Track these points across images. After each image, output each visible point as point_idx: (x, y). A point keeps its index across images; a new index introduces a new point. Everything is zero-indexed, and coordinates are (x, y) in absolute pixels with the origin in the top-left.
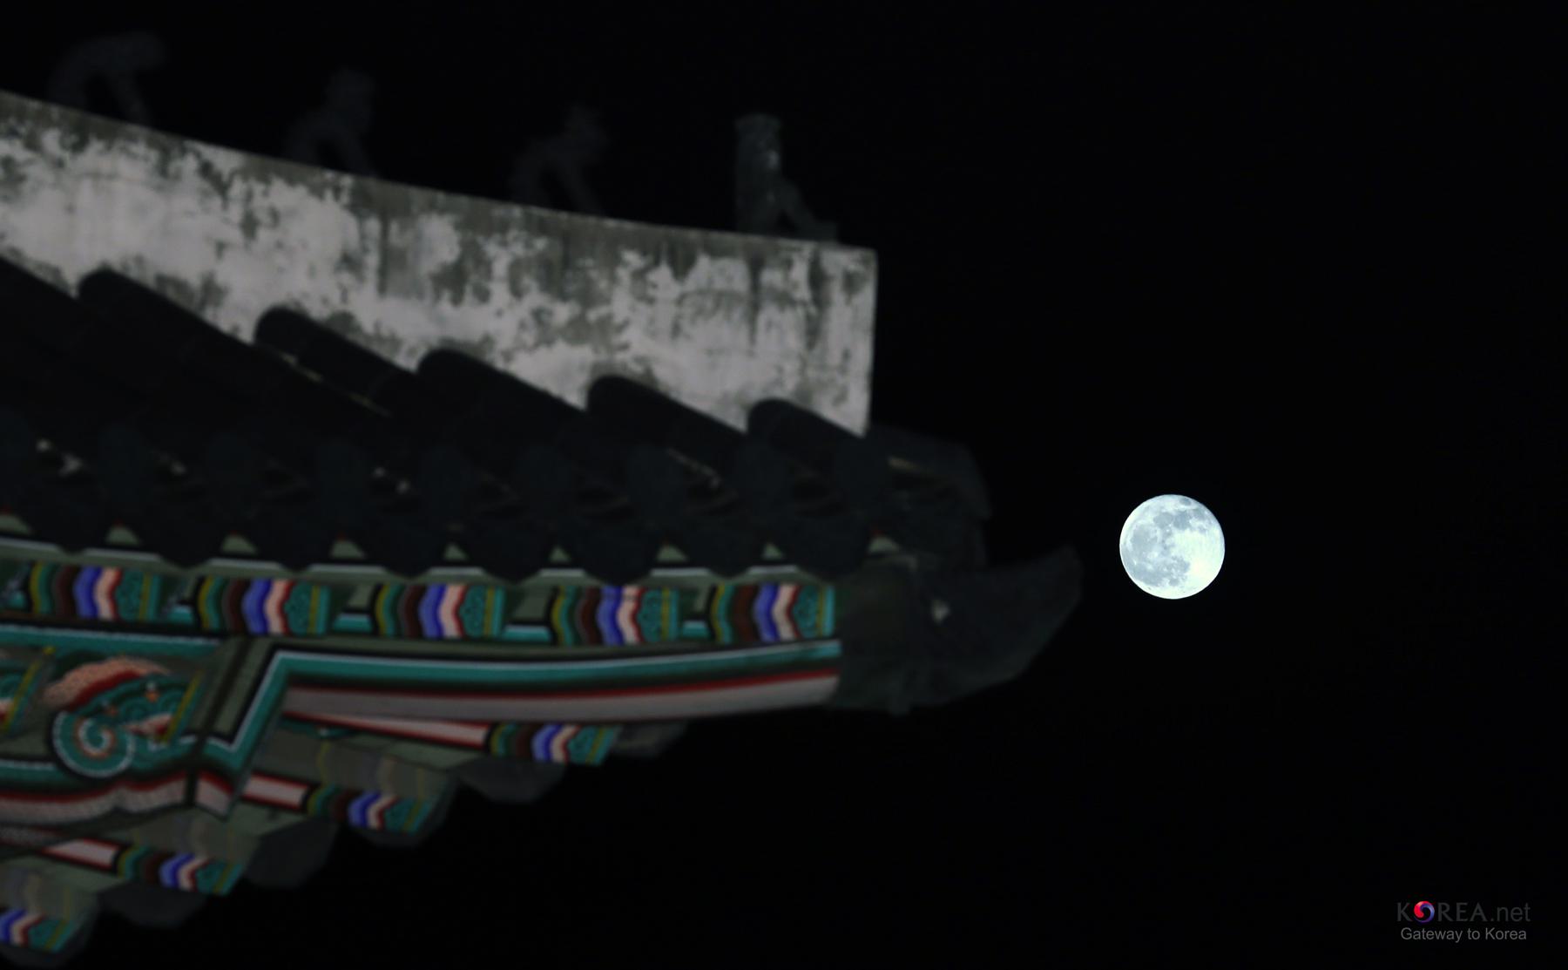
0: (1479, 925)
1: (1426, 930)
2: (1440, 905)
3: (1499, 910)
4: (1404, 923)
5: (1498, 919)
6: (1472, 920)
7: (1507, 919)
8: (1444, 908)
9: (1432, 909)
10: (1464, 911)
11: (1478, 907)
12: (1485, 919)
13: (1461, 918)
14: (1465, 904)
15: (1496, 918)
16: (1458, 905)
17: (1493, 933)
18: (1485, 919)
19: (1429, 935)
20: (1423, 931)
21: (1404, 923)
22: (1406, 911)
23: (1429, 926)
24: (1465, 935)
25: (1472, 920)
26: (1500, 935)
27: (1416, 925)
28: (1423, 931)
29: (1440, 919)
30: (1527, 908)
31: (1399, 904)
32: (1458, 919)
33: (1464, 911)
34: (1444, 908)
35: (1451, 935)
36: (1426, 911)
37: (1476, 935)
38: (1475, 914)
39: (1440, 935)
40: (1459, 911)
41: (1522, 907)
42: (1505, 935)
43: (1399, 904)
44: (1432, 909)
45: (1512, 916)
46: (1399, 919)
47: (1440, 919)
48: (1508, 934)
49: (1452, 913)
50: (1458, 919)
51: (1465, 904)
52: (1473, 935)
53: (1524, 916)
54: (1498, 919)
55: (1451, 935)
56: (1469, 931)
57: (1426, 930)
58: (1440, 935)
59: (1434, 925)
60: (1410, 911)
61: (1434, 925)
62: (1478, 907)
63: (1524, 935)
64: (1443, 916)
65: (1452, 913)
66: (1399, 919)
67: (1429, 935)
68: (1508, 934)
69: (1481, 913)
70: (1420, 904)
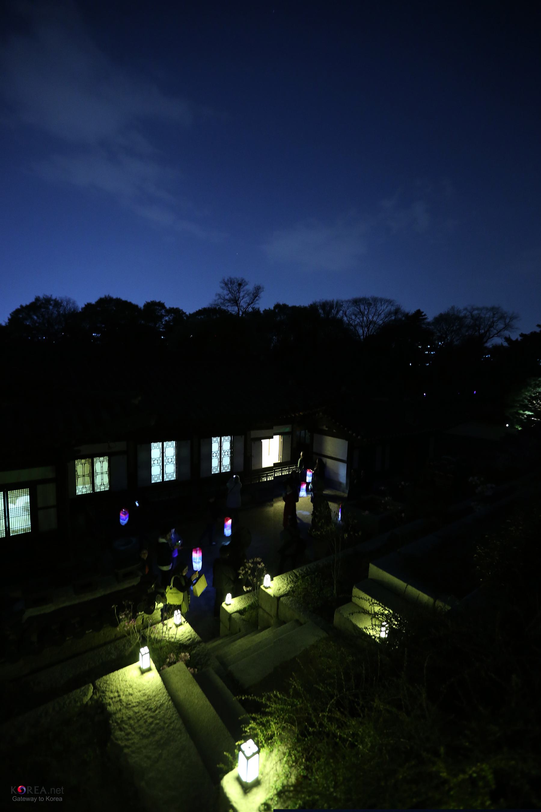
0: (43, 795)
1: (23, 797)
2: (28, 787)
3: (51, 789)
4: (14, 794)
5: (51, 793)
6: (41, 793)
7: (54, 793)
8: (29, 788)
9: (25, 789)
10: (38, 790)
11: (43, 788)
12: (46, 793)
13: (36, 792)
14: (38, 787)
15: (50, 793)
16: (35, 787)
17: (49, 798)
18: (46, 793)
19: (24, 799)
20: (21, 798)
21: (14, 794)
22: (14, 790)
24: (38, 799)
25: (41, 793)
27: (18, 795)
28: (21, 798)
29: (28, 793)
30: (62, 789)
31: (12, 787)
32: (35, 793)
33: (38, 790)
34: (29, 788)
35: (32, 799)
36: (22, 790)
37: (42, 799)
38: (42, 791)
39: (28, 799)
40: (35, 790)
41: (60, 788)
42: (53, 799)
43: (12, 787)
44: (25, 789)
45: (57, 792)
46: (12, 793)
47: (28, 793)
48: (55, 799)
49: (33, 791)
50: (35, 793)
51: (38, 787)
52: (41, 799)
53: (61, 792)
54: (51, 793)
55: (32, 799)
56: (40, 798)
57: (23, 797)
58: (28, 799)
59: (26, 795)
60: (16, 790)
61: (26, 795)
62: (43, 788)
63: (61, 799)
64: (29, 791)
65: (33, 791)
66: (12, 793)
67: (24, 799)
68: (55, 799)
69: (44, 791)
70: (20, 787)
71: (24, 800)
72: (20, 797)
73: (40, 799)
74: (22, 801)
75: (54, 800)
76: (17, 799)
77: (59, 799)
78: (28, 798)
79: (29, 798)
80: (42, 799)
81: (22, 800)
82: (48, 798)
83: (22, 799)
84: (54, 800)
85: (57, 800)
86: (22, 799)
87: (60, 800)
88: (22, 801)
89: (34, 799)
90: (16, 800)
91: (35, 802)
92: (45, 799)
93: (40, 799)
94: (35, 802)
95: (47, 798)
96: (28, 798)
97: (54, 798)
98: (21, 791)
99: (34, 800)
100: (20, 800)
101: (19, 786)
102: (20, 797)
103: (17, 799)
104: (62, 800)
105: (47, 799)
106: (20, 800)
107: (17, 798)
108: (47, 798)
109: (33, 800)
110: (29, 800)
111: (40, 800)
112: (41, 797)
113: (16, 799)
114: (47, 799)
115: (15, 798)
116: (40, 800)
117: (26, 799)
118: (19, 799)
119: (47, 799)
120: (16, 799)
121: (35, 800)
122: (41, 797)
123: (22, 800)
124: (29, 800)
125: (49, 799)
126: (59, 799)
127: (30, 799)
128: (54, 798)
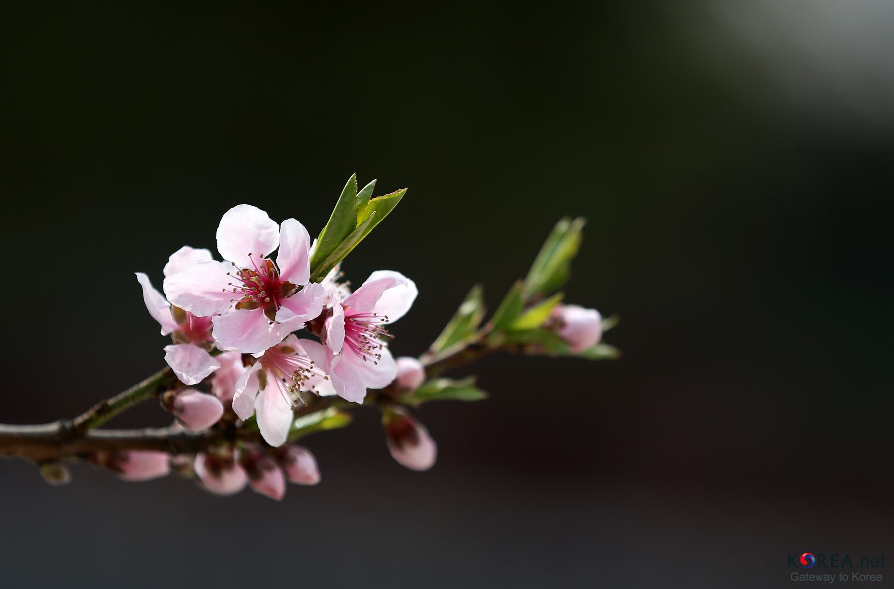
1: (809, 574)
9: (813, 559)
17: (858, 576)
19: (811, 577)
20: (807, 575)
24: (837, 577)
26: (862, 578)
28: (807, 575)
36: (808, 559)
37: (845, 578)
44: (813, 559)
48: (869, 577)
56: (840, 575)
57: (809, 574)
67: (811, 577)
68: (869, 577)
70: (804, 555)
71: (812, 579)
72: (805, 574)
73: (842, 576)
74: (807, 580)
75: (867, 580)
76: (799, 577)
77: (876, 577)
78: (819, 575)
79: (821, 577)
81: (808, 578)
82: (855, 576)
83: (808, 576)
84: (867, 580)
85: (872, 579)
86: (808, 576)
87: (879, 579)
88: (807, 580)
89: (830, 576)
90: (796, 578)
91: (831, 582)
92: (850, 576)
94: (831, 582)
95: (854, 574)
96: (819, 575)
97: (867, 576)
98: (805, 563)
100: (804, 579)
101: (815, 556)
102: (805, 574)
103: (799, 577)
104: (881, 579)
105: (855, 578)
108: (854, 574)
110: (821, 580)
111: (842, 579)
112: (842, 574)
113: (798, 577)
114: (855, 578)
115: (796, 575)
116: (842, 579)
117: (815, 578)
118: (804, 577)
119: (853, 577)
120: (798, 577)
121: (833, 580)
122: (842, 574)
123: (808, 578)
124: (821, 580)
125: (859, 579)
126: (876, 577)
127: (823, 578)
128: (867, 576)
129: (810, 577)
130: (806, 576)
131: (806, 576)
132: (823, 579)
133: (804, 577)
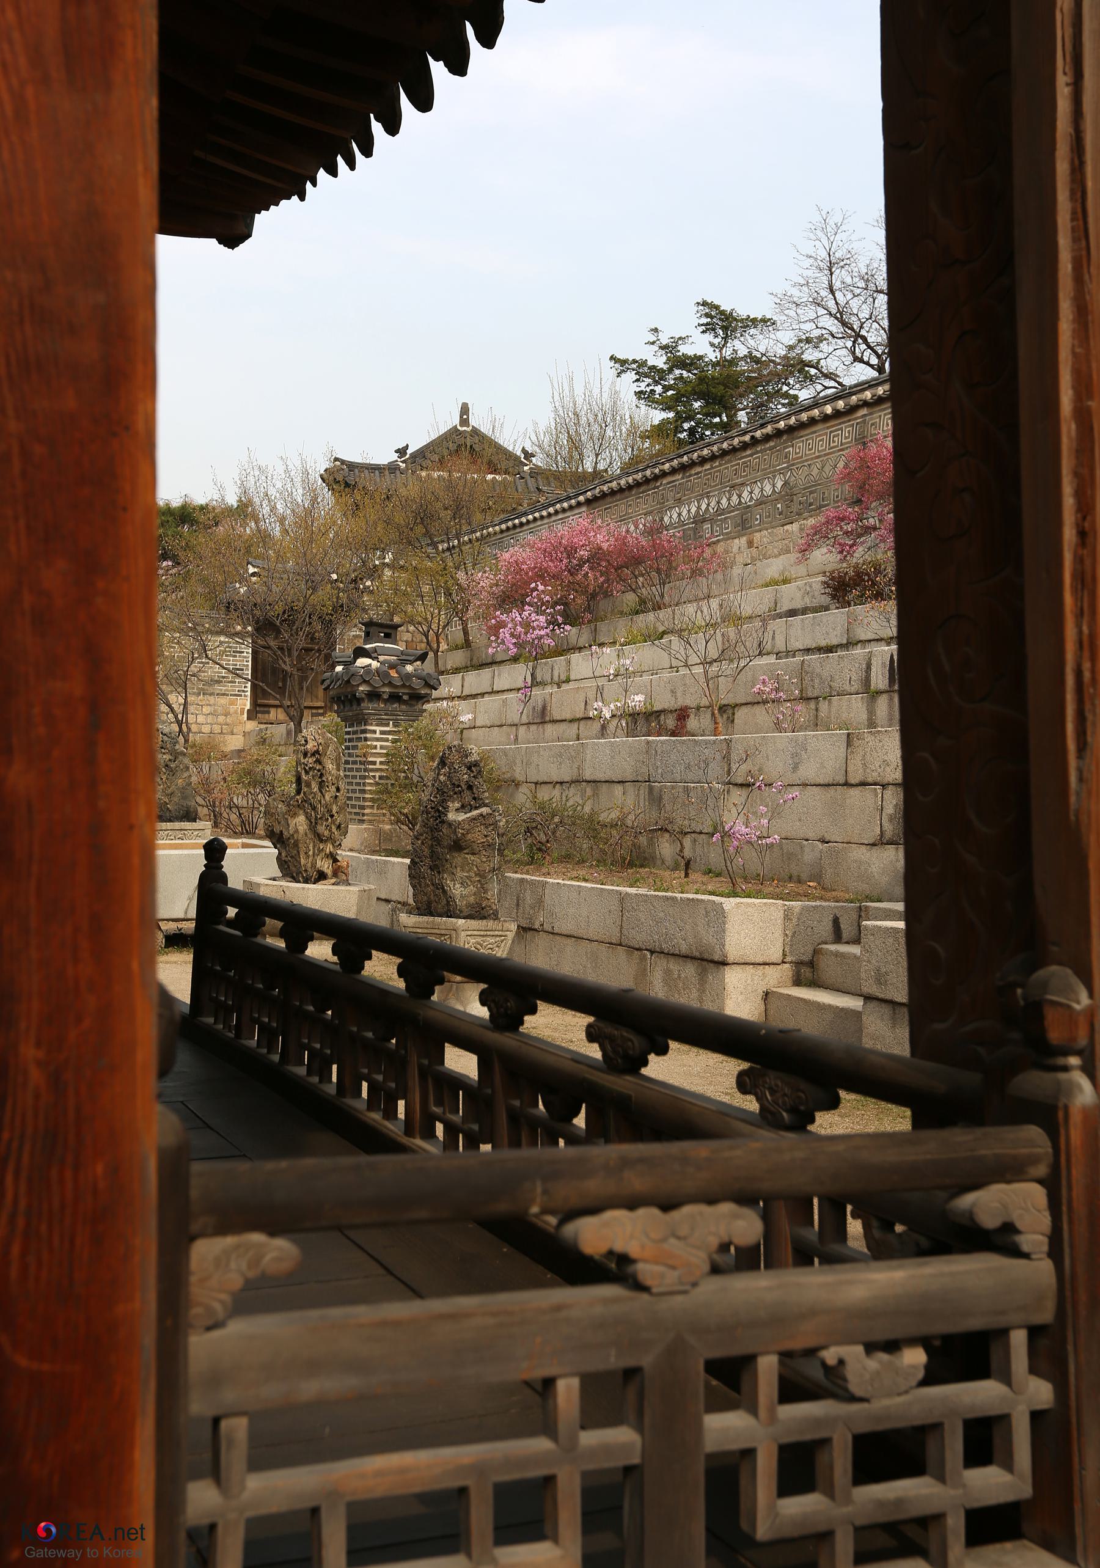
1: (49, 1549)
9: (53, 1529)
17: (111, 1551)
19: (51, 1553)
20: (46, 1550)
23: (50, 1546)
24: (84, 1555)
26: (117, 1553)
27: (39, 1544)
28: (46, 1550)
36: (48, 1531)
37: (95, 1553)
44: (53, 1529)
48: (125, 1552)
56: (88, 1550)
57: (49, 1549)
67: (51, 1553)
68: (125, 1552)
70: (43, 1524)
71: (52, 1555)
73: (90, 1552)
76: (36, 1553)
78: (62, 1551)
80: (95, 1553)
82: (108, 1551)
83: (48, 1552)
86: (48, 1552)
93: (90, 1552)
96: (62, 1551)
98: (43, 1535)
99: (76, 1557)
100: (42, 1556)
102: (43, 1549)
103: (36, 1553)
106: (42, 1556)
107: (35, 1551)
109: (73, 1556)
113: (34, 1553)
114: (107, 1554)
118: (40, 1553)
120: (34, 1553)
121: (79, 1556)
125: (112, 1554)
129: (50, 1553)
130: (44, 1552)
131: (44, 1552)
132: (66, 1555)
133: (40, 1553)
